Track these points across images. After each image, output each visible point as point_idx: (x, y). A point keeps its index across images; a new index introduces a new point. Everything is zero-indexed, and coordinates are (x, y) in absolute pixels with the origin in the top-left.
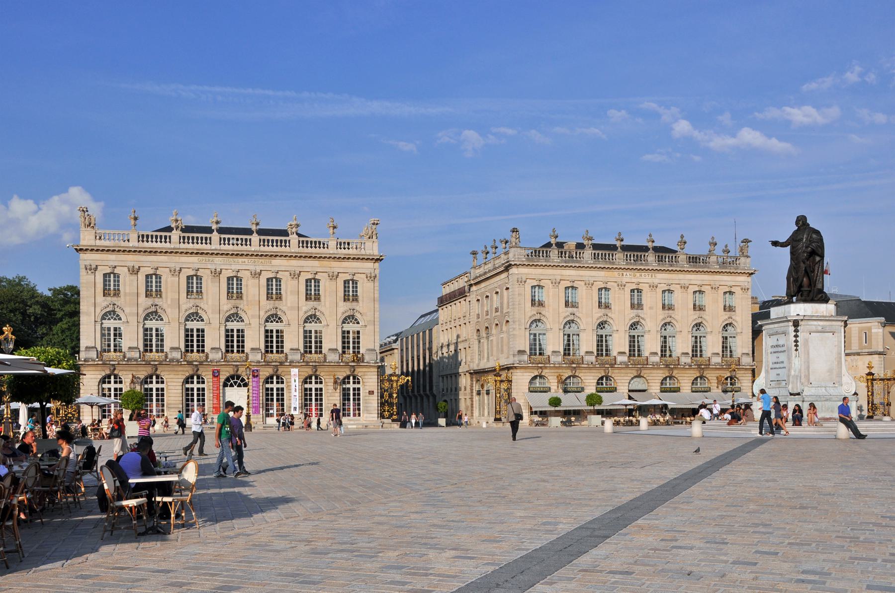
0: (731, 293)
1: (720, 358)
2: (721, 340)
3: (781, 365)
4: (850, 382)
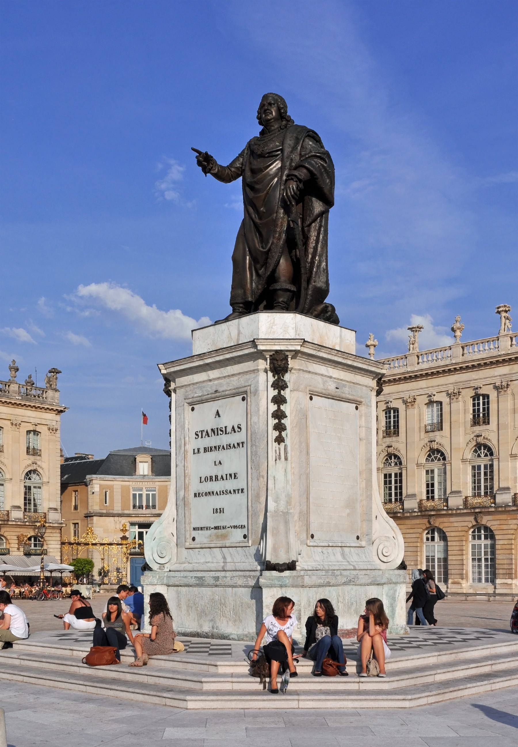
0: (36, 433)
1: (22, 512)
2: (23, 490)
3: (230, 485)
4: (391, 534)
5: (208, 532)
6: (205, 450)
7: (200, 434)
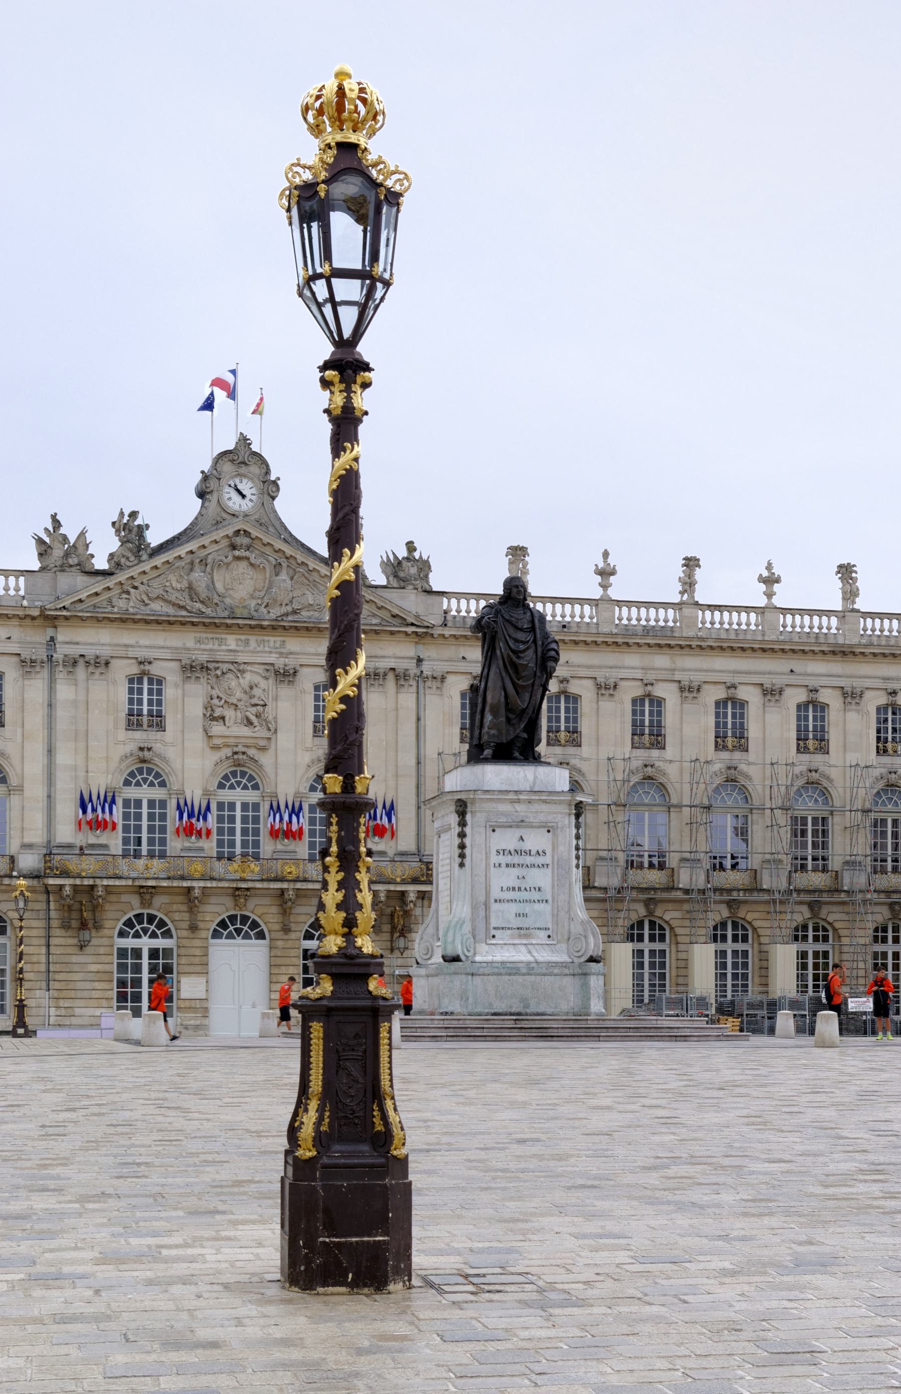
3: (536, 896)
5: (509, 932)
6: (507, 865)
7: (502, 852)
